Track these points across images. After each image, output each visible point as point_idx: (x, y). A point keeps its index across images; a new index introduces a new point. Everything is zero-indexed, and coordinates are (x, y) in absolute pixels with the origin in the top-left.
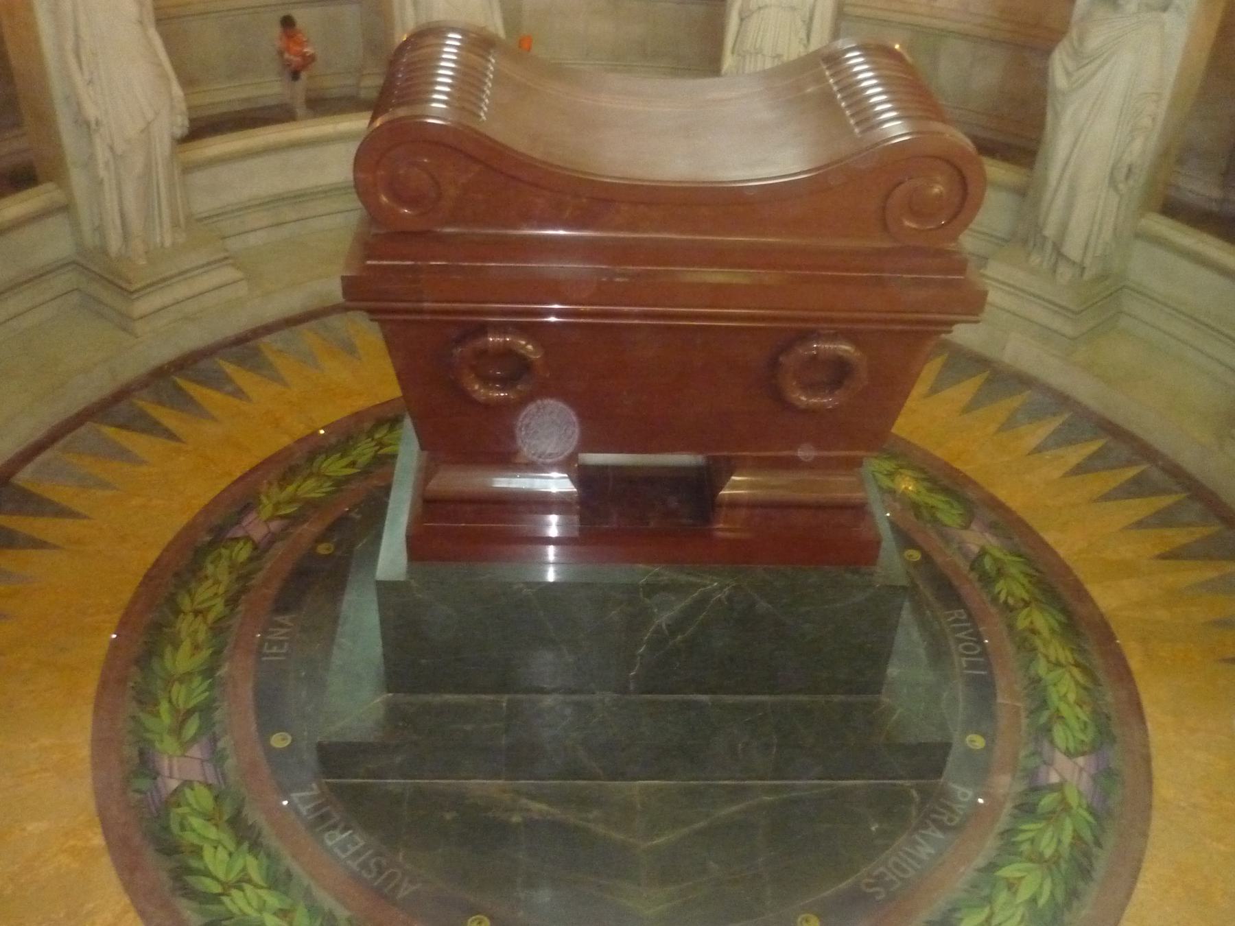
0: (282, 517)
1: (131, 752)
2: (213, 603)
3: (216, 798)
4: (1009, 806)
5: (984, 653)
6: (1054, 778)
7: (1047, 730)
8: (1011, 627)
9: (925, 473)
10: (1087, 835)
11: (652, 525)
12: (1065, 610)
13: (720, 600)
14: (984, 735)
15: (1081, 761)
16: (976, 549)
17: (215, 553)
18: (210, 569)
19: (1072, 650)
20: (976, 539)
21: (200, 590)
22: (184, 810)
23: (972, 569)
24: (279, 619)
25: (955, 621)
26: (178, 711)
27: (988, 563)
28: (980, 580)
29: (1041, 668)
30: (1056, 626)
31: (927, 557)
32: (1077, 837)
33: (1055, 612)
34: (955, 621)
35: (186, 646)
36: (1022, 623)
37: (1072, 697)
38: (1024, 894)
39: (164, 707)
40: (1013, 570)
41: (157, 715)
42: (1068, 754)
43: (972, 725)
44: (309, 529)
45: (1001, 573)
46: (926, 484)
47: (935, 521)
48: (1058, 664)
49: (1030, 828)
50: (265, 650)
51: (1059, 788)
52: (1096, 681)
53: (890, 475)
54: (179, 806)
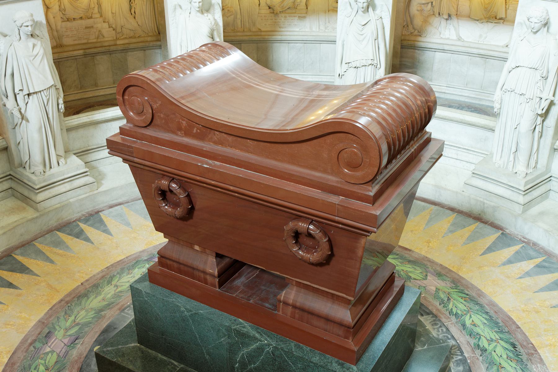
1: (46, 330)
2: (123, 284)
3: (56, 362)
9: (515, 347)
11: (251, 301)
13: (268, 352)
17: (143, 265)
18: (137, 270)
21: (126, 277)
22: (43, 362)
26: (75, 321)
35: (100, 298)
39: (72, 318)
41: (67, 321)
50: (126, 311)
54: (42, 359)
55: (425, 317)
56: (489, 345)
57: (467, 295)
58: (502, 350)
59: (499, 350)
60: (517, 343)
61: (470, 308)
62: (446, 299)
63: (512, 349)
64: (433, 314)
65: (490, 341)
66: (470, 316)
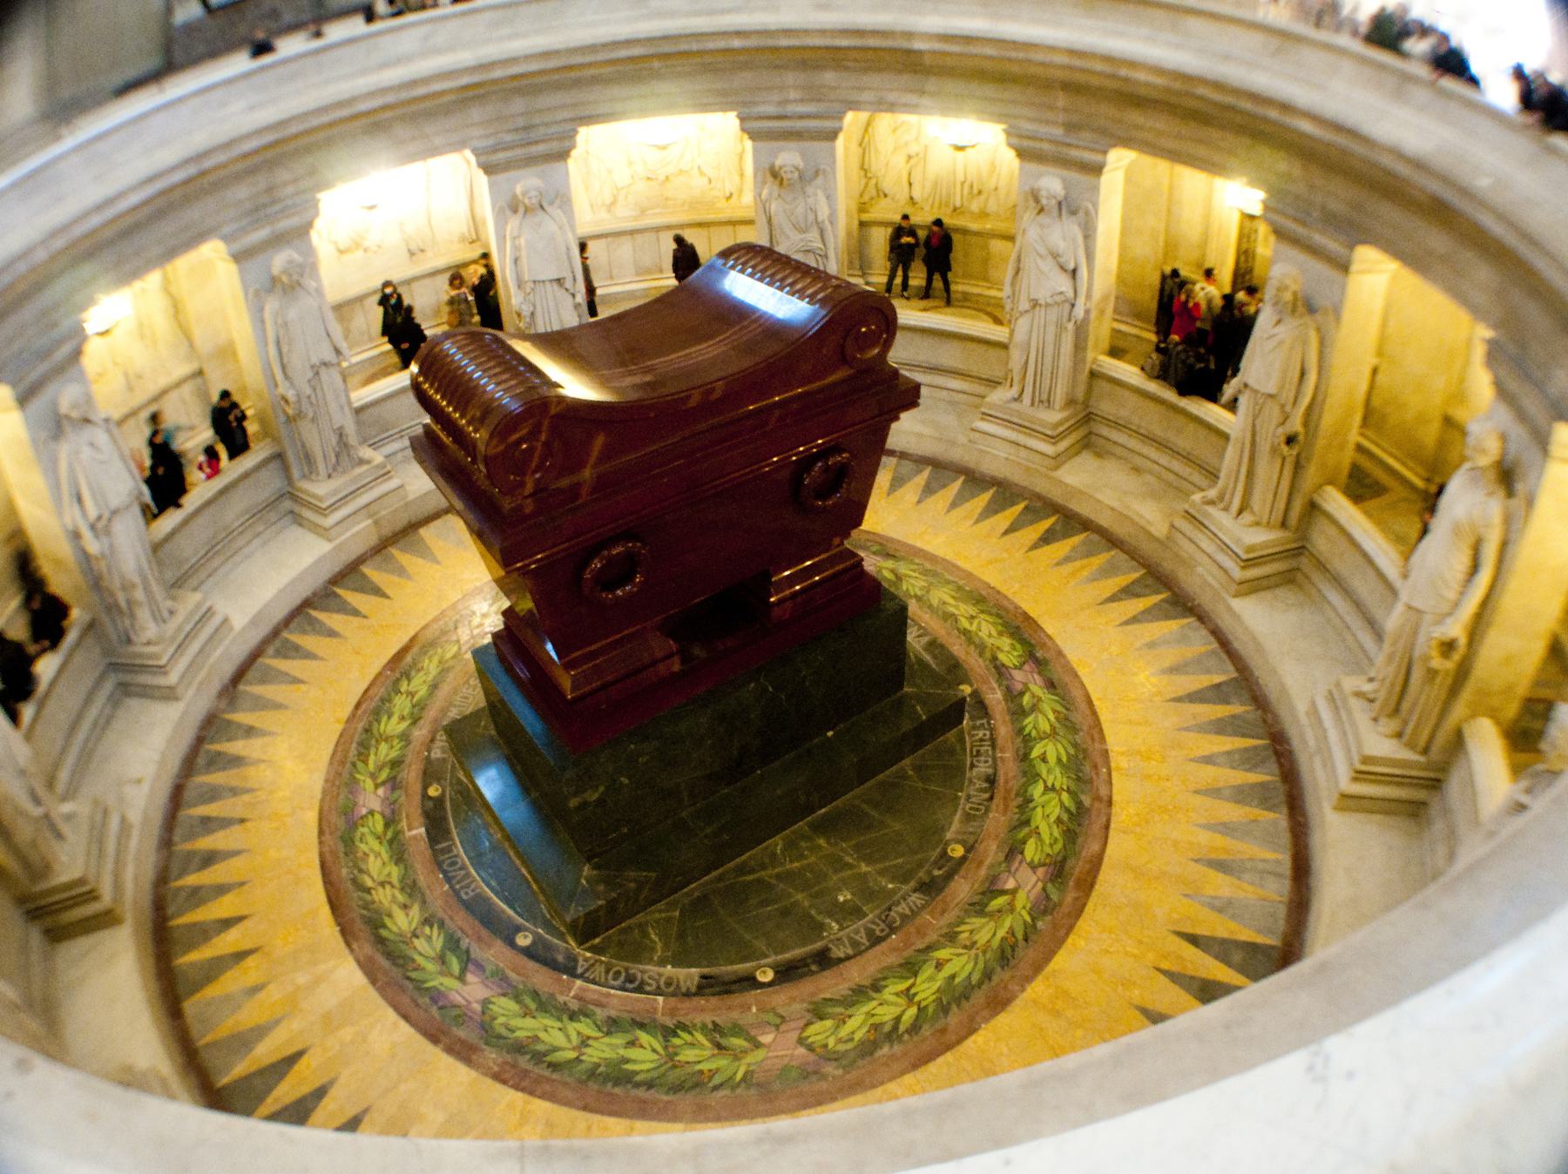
0: (1022, 694)
4: (408, 760)
5: (439, 865)
6: (381, 791)
7: (387, 825)
8: (424, 902)
9: (550, 1065)
10: (360, 765)
12: (381, 941)
14: (430, 798)
15: (364, 811)
16: (470, 977)
19: (373, 902)
20: (471, 992)
23: (468, 951)
24: (926, 639)
25: (468, 886)
27: (455, 966)
28: (458, 941)
29: (395, 872)
30: (387, 921)
31: (511, 943)
32: (365, 762)
33: (391, 937)
34: (468, 886)
36: (415, 911)
37: (372, 858)
38: (395, 719)
40: (431, 967)
42: (371, 813)
43: (439, 801)
44: (995, 697)
45: (442, 959)
46: (540, 1047)
47: (517, 998)
48: (382, 884)
49: (394, 754)
51: (377, 786)
52: (354, 881)
53: (585, 1042)
55: (697, 979)
56: (579, 1033)
57: (716, 1088)
58: (556, 1043)
59: (556, 1038)
60: (555, 1076)
61: (675, 1067)
62: (724, 1042)
63: (548, 1059)
64: (695, 994)
65: (585, 1042)
66: (654, 1051)
